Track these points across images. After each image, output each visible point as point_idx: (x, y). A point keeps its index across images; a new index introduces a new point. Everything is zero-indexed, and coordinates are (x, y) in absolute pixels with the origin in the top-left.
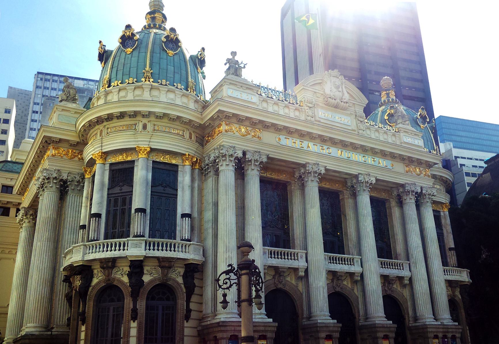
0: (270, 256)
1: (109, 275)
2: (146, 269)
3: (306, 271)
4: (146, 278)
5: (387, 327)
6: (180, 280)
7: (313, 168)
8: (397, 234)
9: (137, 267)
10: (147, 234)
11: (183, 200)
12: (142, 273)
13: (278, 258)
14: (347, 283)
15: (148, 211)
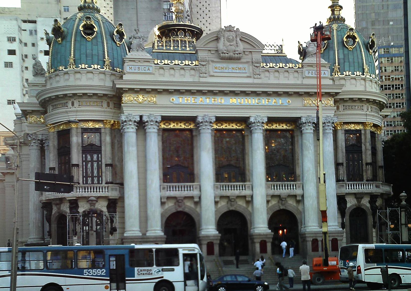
0: (169, 189)
1: (59, 209)
2: (81, 204)
3: (200, 198)
4: (81, 210)
5: (264, 235)
6: (105, 209)
7: (203, 119)
8: (298, 159)
9: (74, 204)
10: (81, 181)
11: (105, 154)
12: (77, 207)
13: (176, 190)
14: (241, 203)
15: (81, 164)
